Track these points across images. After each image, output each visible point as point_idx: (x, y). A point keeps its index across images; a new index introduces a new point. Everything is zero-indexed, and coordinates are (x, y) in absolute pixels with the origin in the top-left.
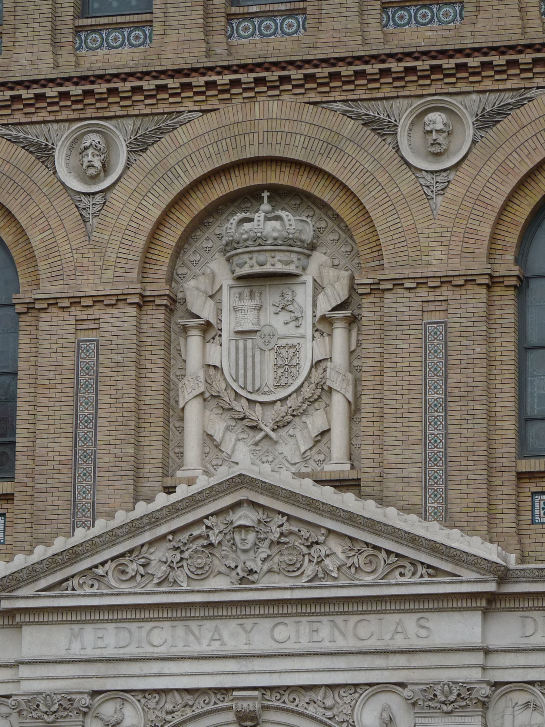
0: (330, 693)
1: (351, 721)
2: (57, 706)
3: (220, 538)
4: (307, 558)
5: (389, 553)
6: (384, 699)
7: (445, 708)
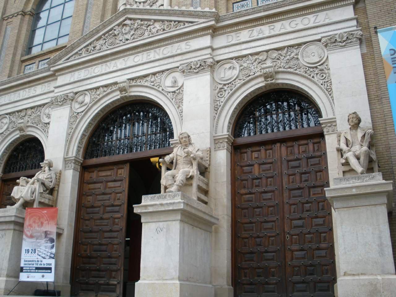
0: (153, 76)
1: (160, 85)
2: (63, 99)
3: (118, 32)
4: (146, 31)
5: (175, 21)
6: (173, 74)
7: (195, 71)
